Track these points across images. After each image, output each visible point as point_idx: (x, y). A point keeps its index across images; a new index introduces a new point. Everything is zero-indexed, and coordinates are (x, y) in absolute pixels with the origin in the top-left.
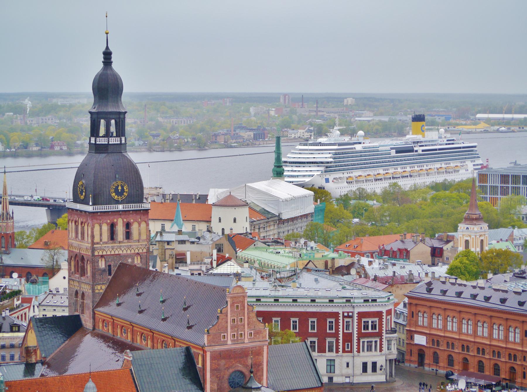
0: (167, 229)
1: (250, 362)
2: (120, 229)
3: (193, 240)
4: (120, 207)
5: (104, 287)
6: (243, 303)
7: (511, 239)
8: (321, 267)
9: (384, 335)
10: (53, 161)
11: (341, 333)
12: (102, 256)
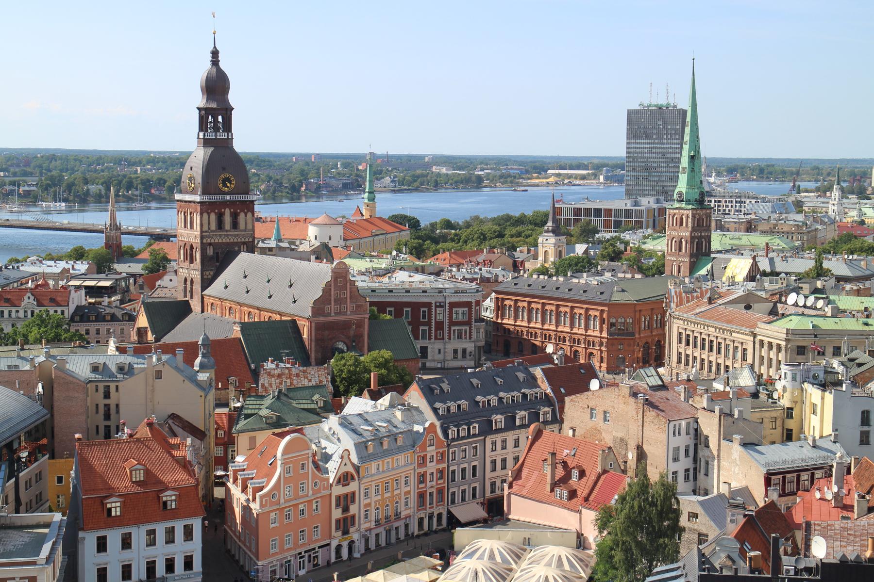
2: (227, 219)
3: (293, 247)
4: (228, 198)
5: (212, 273)
11: (433, 321)
12: (210, 244)
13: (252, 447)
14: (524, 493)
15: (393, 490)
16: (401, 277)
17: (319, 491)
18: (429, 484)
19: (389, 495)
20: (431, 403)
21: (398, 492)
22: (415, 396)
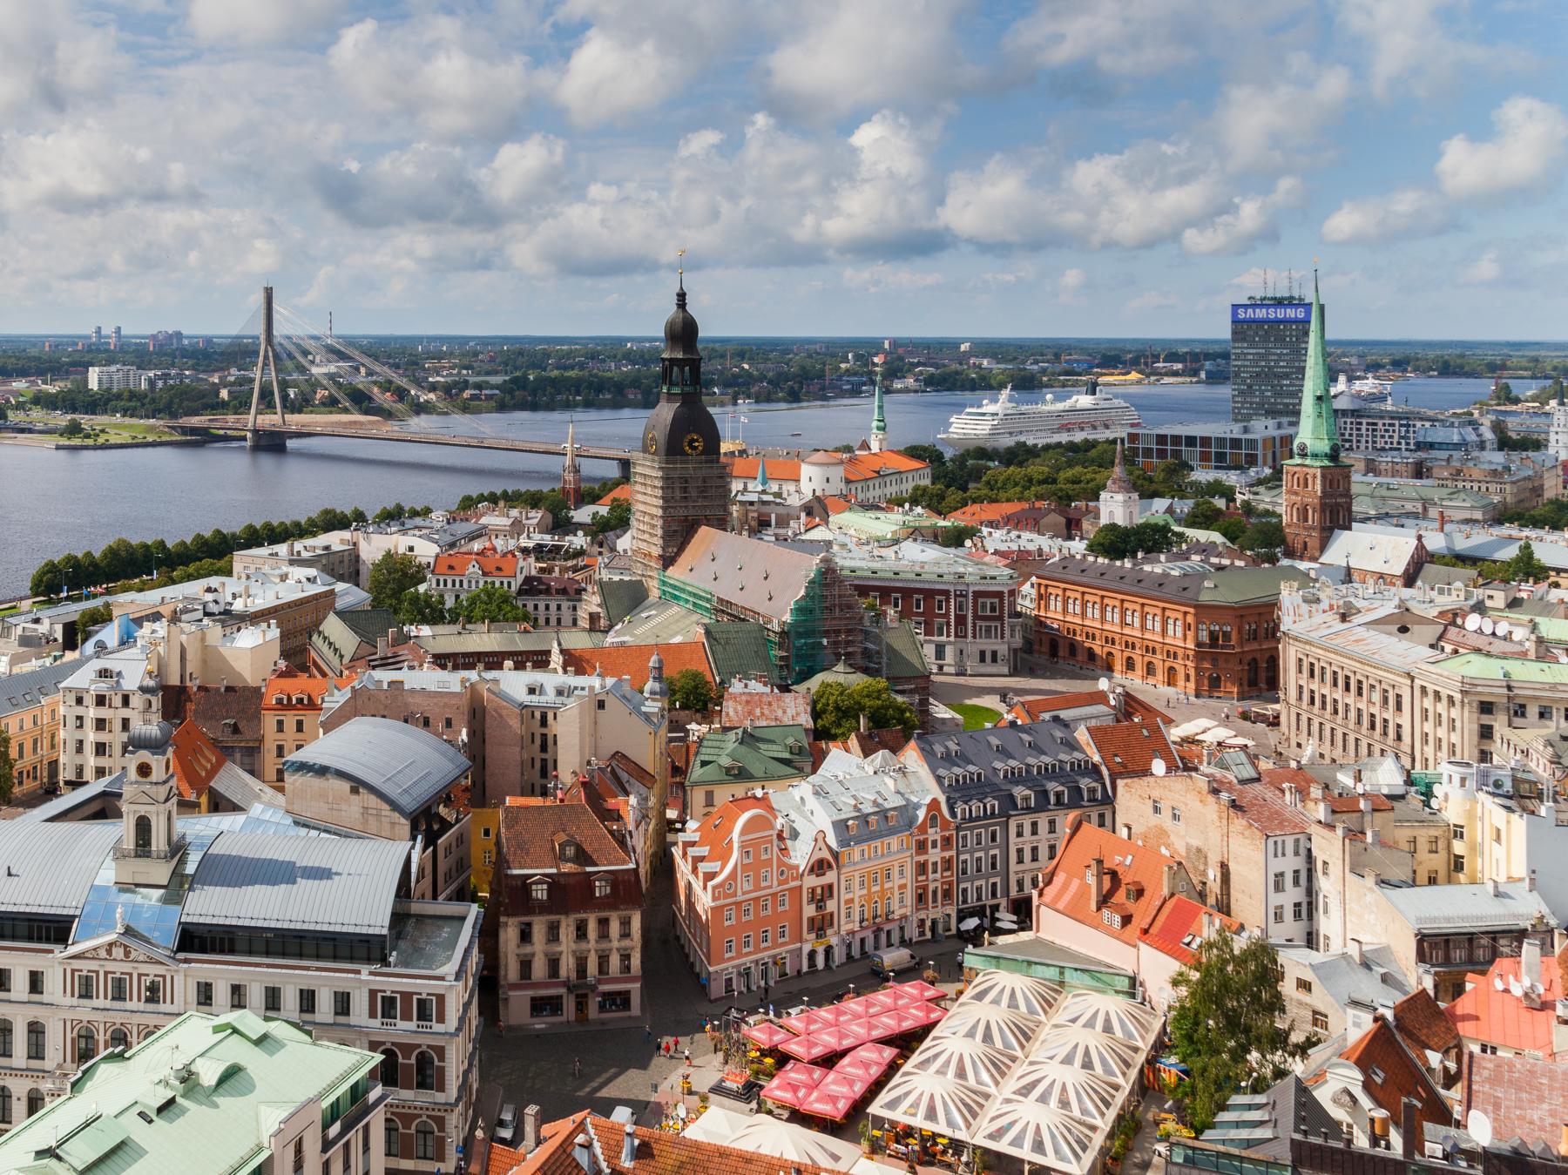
13: (709, 801)
14: (1060, 906)
15: (882, 884)
18: (931, 876)
19: (877, 888)
20: (933, 771)
21: (889, 885)
22: (911, 756)
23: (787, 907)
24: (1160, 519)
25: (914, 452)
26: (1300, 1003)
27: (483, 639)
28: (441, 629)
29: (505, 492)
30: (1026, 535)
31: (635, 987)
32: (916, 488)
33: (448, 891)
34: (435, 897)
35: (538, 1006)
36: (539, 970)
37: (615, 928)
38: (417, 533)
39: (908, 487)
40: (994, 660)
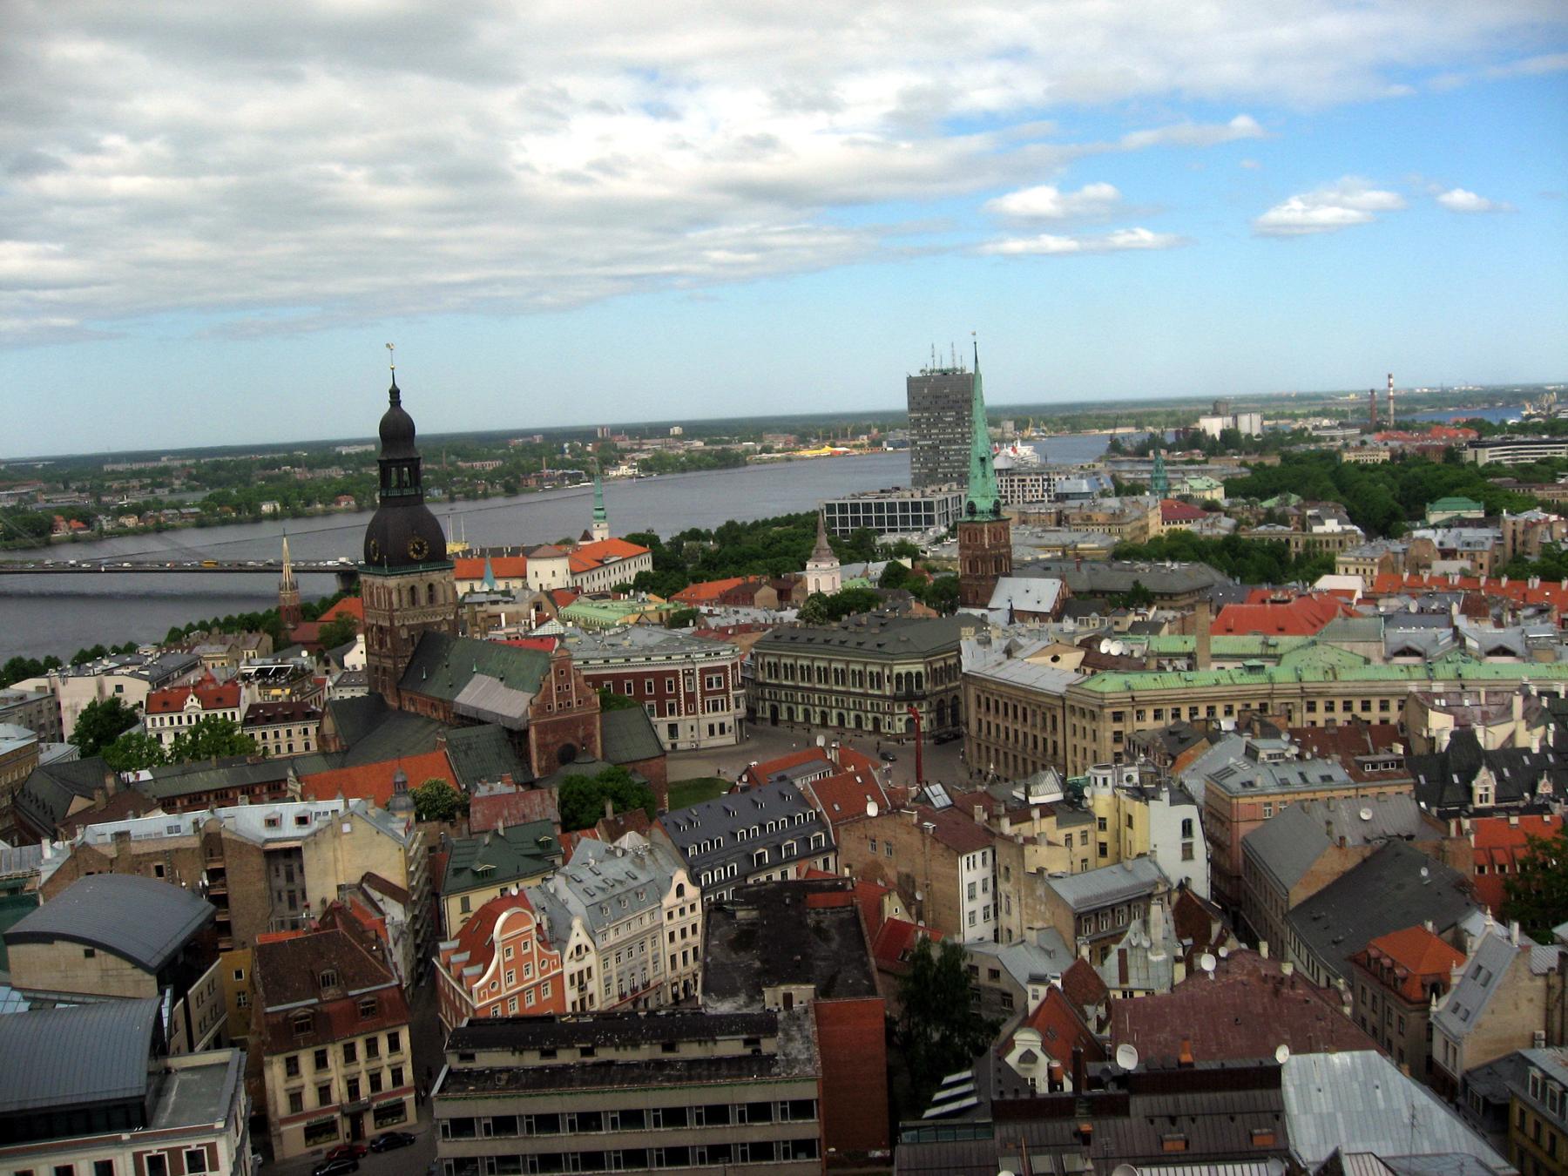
0: (477, 589)
1: (581, 733)
6: (567, 666)
7: (866, 574)
8: (657, 621)
9: (731, 693)
10: (339, 521)
16: (640, 637)
17: (548, 970)
23: (549, 995)
24: (857, 584)
25: (636, 539)
26: (992, 990)
27: (209, 778)
28: (164, 771)
29: (216, 620)
30: (743, 610)
31: (409, 1098)
32: (639, 574)
33: (205, 1040)
34: (191, 1049)
35: (312, 1133)
36: (310, 1100)
37: (383, 1045)
38: (126, 671)
39: (629, 574)
40: (722, 731)
